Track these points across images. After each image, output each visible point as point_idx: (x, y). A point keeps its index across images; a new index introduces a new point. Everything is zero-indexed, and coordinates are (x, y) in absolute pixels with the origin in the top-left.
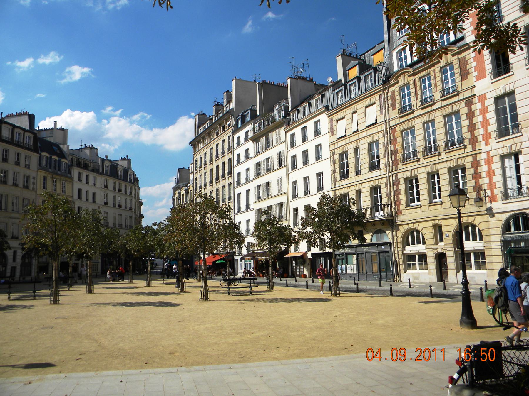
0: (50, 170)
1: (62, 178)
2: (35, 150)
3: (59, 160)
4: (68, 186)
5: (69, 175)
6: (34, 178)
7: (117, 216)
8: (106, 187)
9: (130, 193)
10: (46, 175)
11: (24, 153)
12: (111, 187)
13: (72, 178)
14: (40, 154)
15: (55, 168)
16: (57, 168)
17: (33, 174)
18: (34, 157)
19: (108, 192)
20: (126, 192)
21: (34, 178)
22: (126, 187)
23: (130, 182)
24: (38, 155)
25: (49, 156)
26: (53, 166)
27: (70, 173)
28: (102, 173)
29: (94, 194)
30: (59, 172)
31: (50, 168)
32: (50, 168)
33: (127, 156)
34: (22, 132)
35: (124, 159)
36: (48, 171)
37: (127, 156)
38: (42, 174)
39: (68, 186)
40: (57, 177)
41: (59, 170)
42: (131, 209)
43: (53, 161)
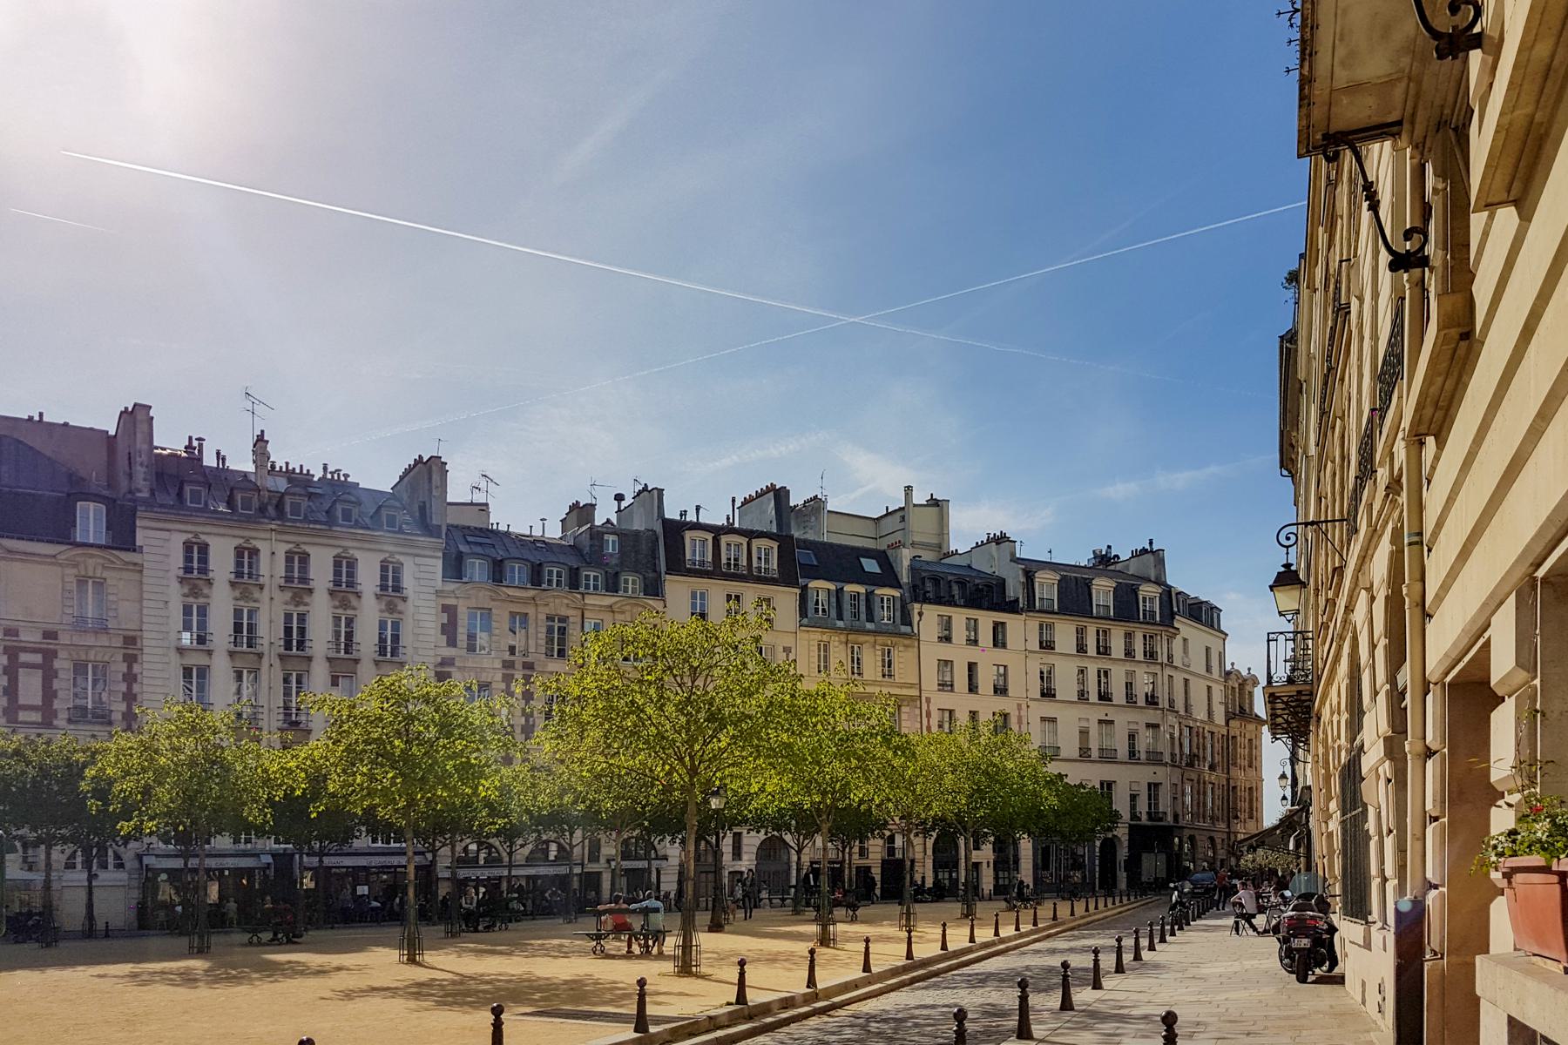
0: (840, 624)
1: (880, 639)
2: (789, 574)
3: (869, 595)
4: (903, 659)
5: (904, 629)
6: (787, 650)
7: (1094, 730)
8: (1047, 646)
9: (1151, 655)
10: (825, 638)
11: (751, 593)
12: (959, 632)
13: (913, 636)
14: (804, 588)
15: (856, 615)
16: (863, 616)
17: (788, 641)
18: (785, 600)
19: (1050, 659)
20: (1129, 653)
21: (787, 650)
22: (1129, 636)
23: (1149, 620)
24: (798, 591)
25: (832, 586)
26: (847, 614)
27: (906, 620)
28: (1028, 605)
29: (972, 667)
30: (869, 626)
31: (840, 617)
32: (840, 617)
33: (1151, 543)
34: (744, 541)
35: (1144, 551)
36: (834, 628)
37: (1151, 543)
38: (816, 636)
39: (903, 659)
40: (862, 638)
41: (870, 618)
42: (1152, 700)
43: (847, 598)
